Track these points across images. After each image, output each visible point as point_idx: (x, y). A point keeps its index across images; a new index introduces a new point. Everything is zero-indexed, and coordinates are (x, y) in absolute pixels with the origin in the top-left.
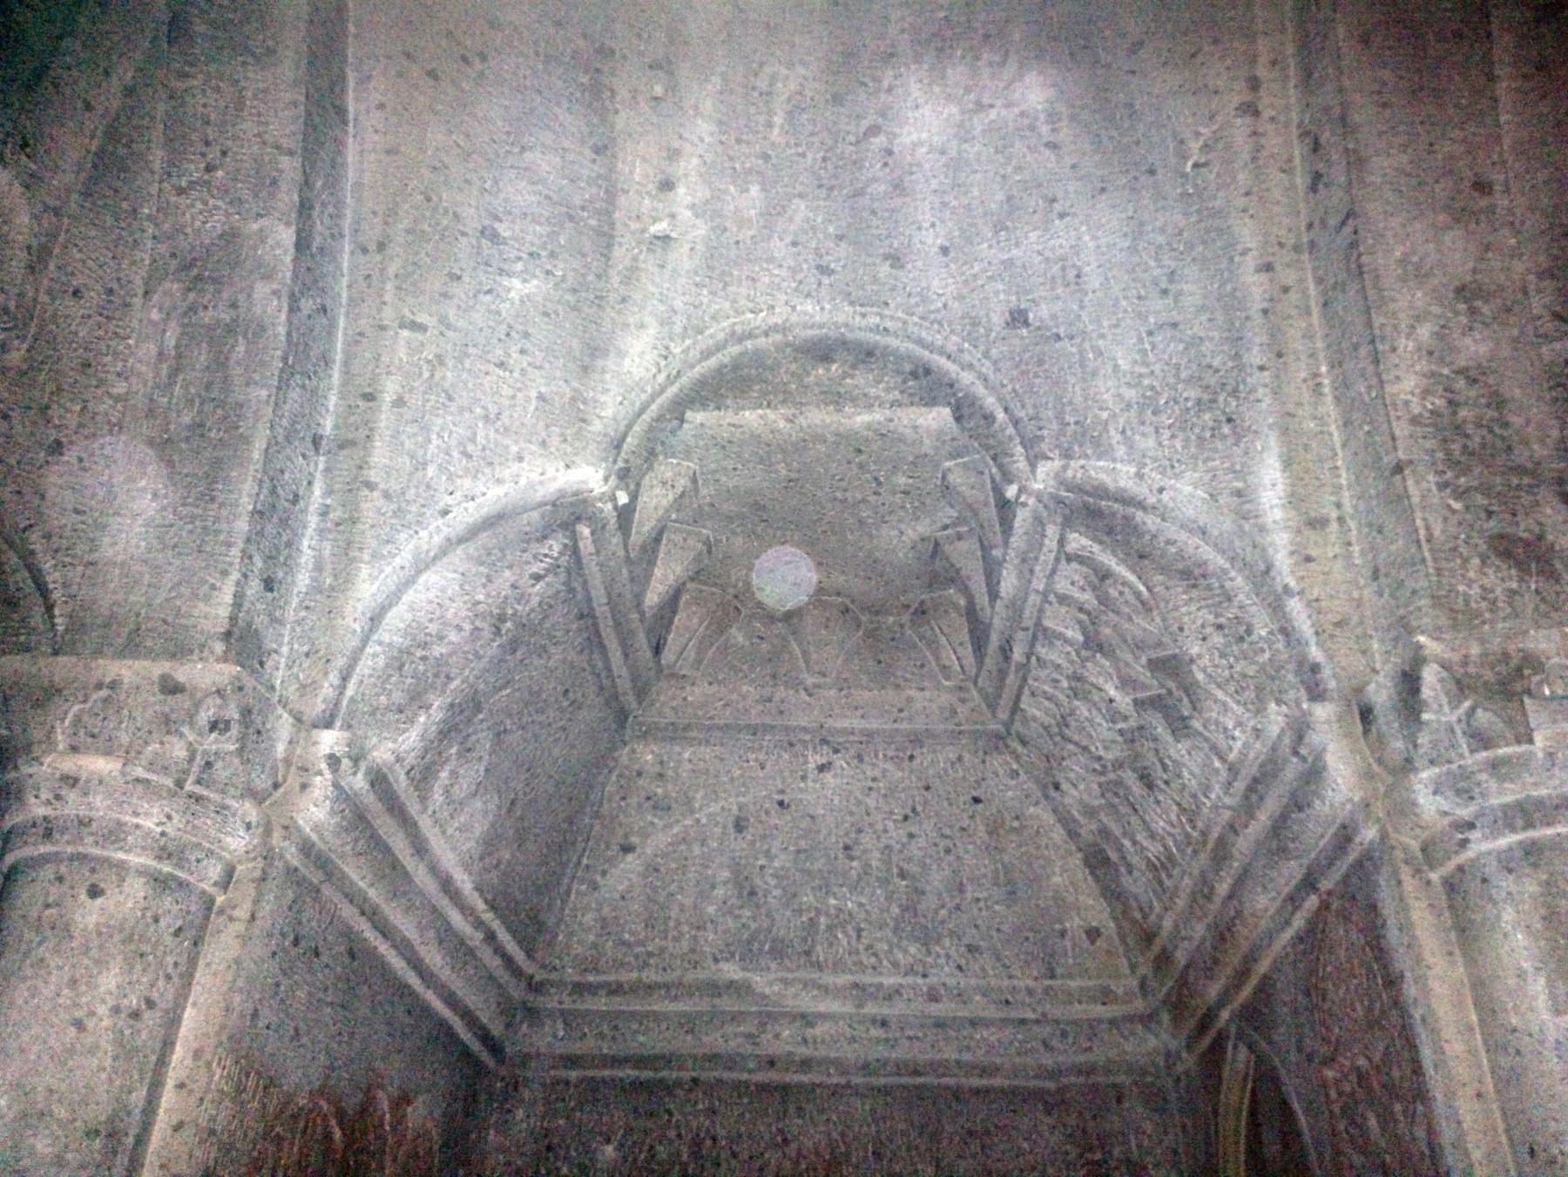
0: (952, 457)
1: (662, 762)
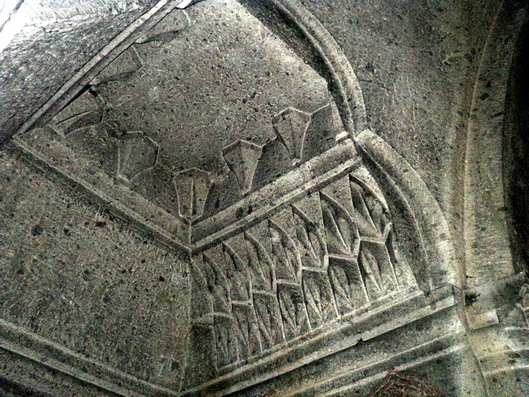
0: (298, 107)
1: (14, 172)
